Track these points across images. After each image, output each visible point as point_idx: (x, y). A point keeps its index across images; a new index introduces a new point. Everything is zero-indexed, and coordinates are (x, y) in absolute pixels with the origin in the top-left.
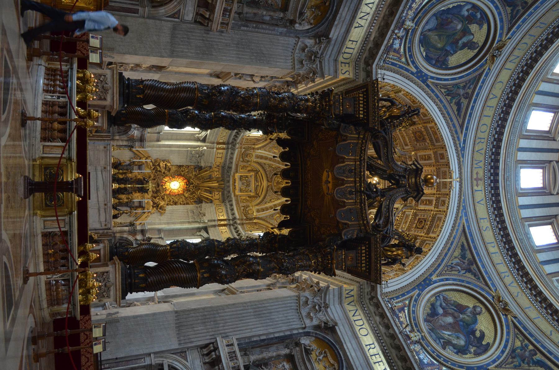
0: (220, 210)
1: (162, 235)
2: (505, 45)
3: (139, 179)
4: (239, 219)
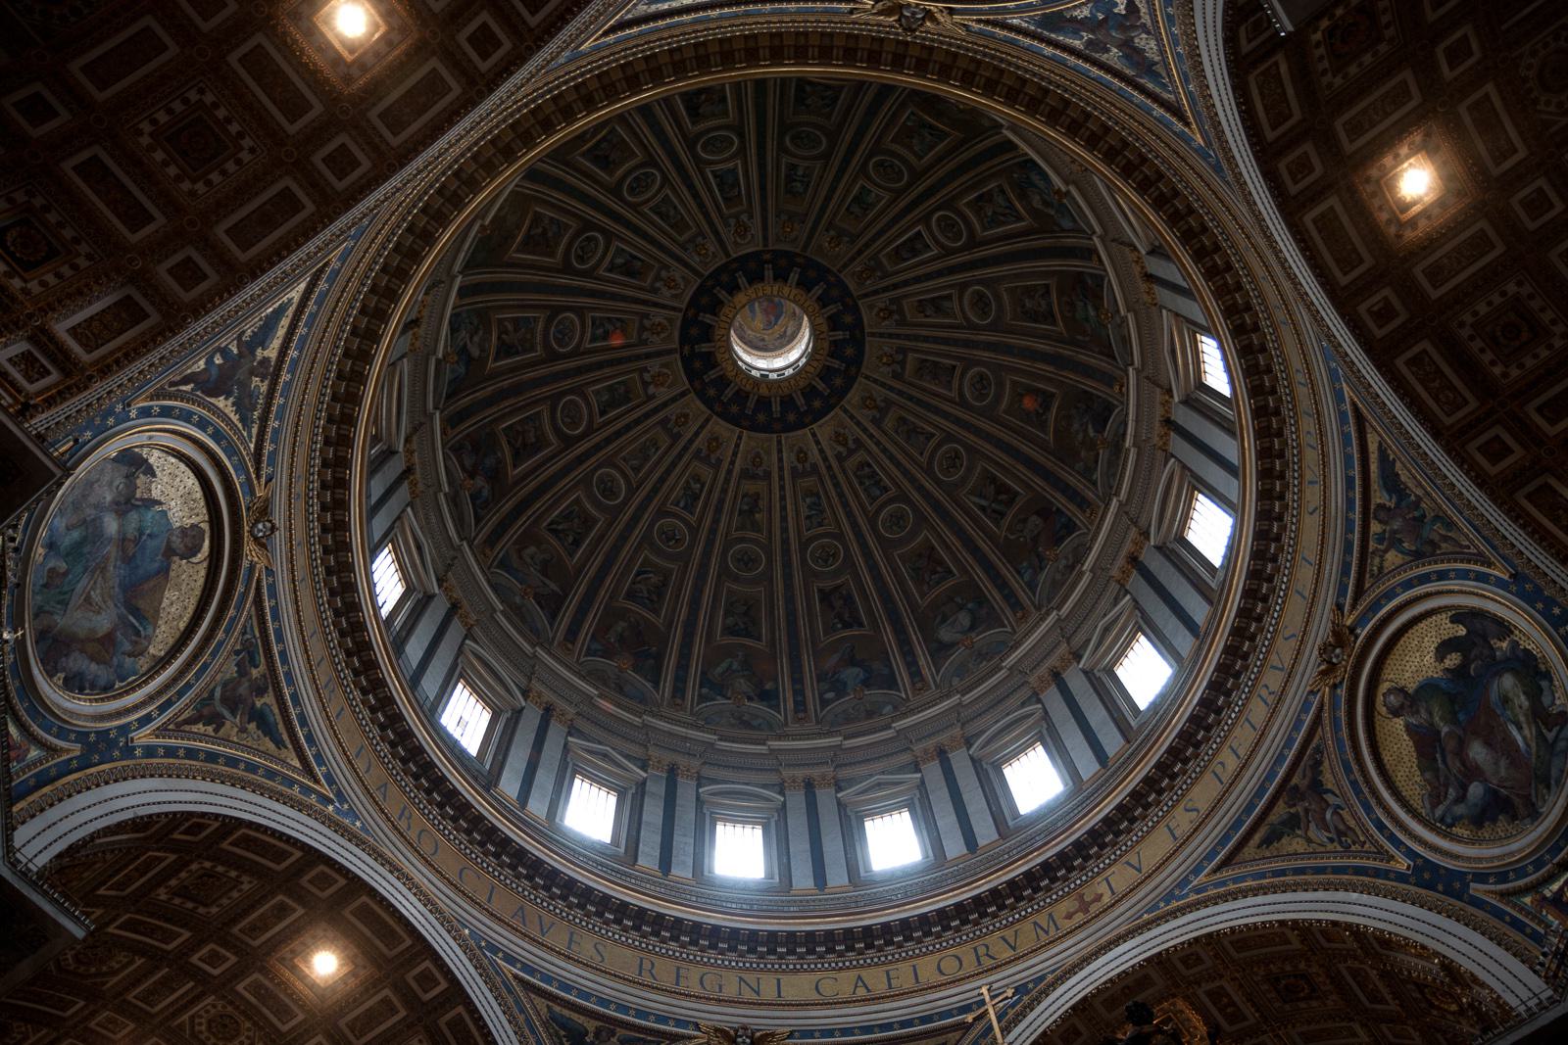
2: (717, 1030)
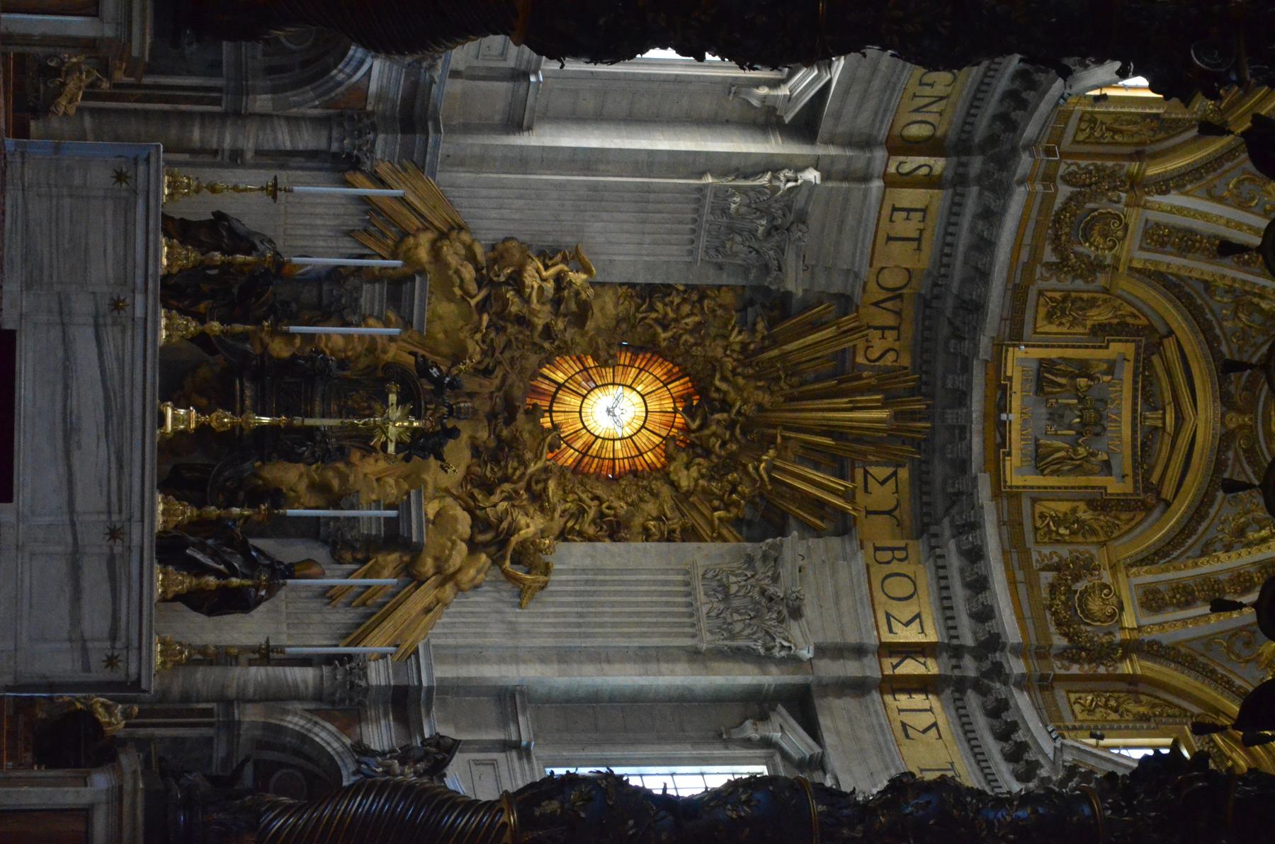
0: (900, 587)
1: (524, 730)
3: (388, 366)
4: (1019, 651)
